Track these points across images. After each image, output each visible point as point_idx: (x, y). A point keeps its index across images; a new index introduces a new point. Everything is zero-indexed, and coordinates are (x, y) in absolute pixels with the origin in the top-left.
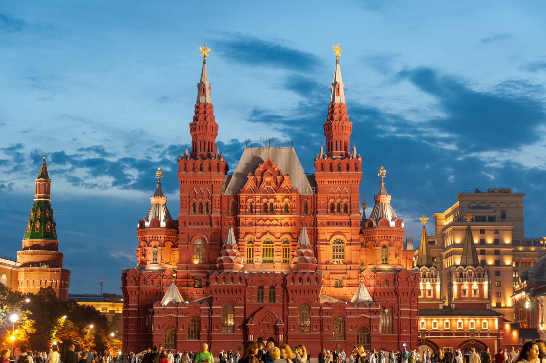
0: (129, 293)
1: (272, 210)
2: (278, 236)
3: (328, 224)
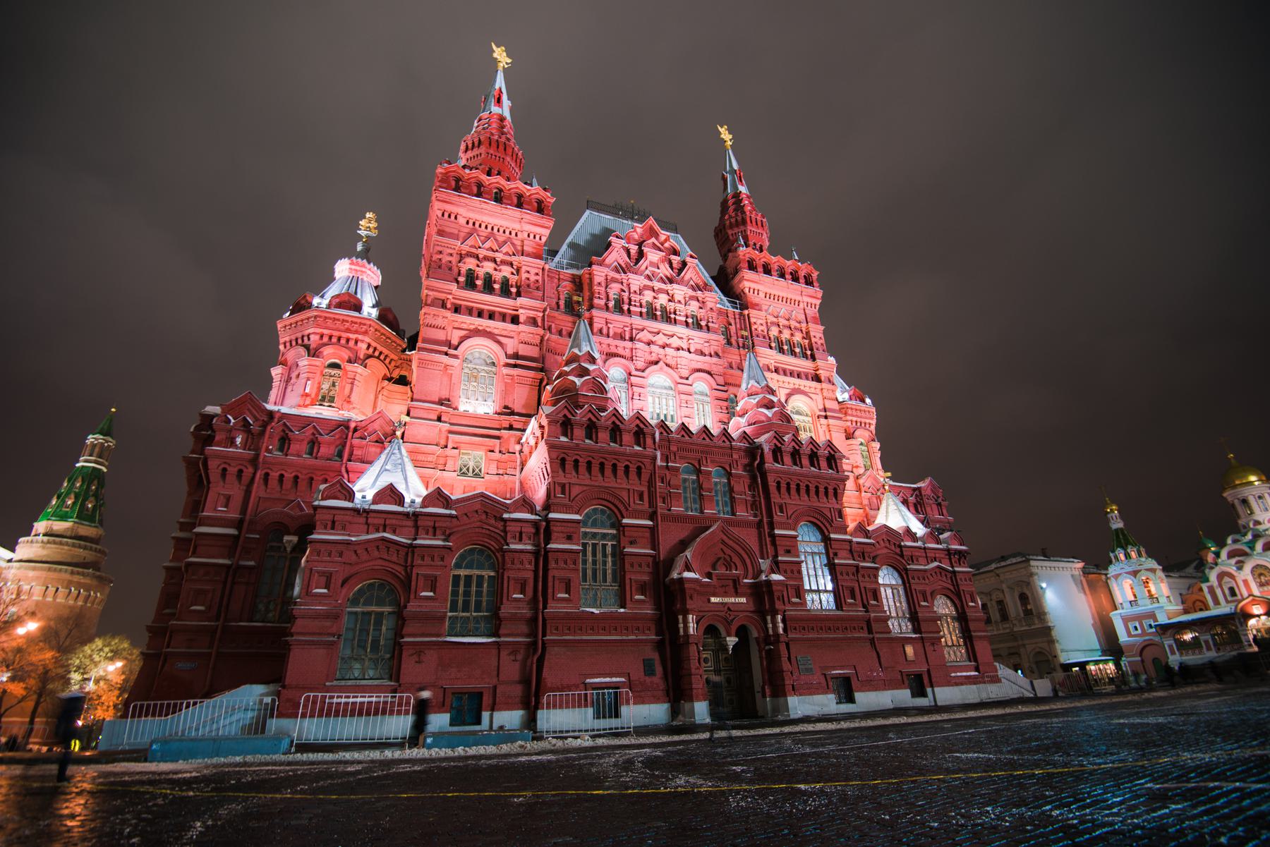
0: (214, 474)
1: (668, 317)
2: (685, 373)
3: (777, 371)
